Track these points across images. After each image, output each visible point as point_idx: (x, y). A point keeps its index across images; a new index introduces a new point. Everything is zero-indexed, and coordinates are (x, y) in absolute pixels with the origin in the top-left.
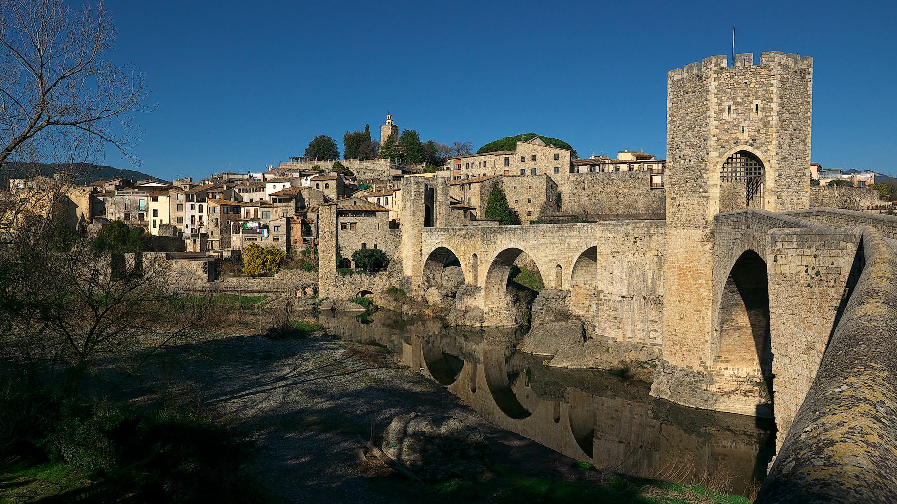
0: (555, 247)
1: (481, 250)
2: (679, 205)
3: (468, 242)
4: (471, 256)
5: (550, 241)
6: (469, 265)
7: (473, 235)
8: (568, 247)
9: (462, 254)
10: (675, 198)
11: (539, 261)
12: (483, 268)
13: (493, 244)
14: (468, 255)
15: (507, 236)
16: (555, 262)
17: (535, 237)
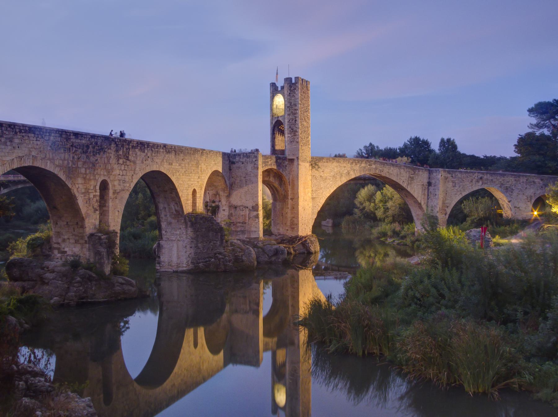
0: (192, 170)
1: (113, 174)
2: (303, 150)
3: (92, 159)
4: (99, 184)
5: (189, 164)
6: (95, 199)
7: (101, 150)
8: (201, 172)
9: (80, 180)
10: (301, 146)
11: (180, 185)
12: (117, 201)
13: (132, 164)
14: (92, 183)
15: (149, 154)
16: (192, 186)
17: (177, 159)
